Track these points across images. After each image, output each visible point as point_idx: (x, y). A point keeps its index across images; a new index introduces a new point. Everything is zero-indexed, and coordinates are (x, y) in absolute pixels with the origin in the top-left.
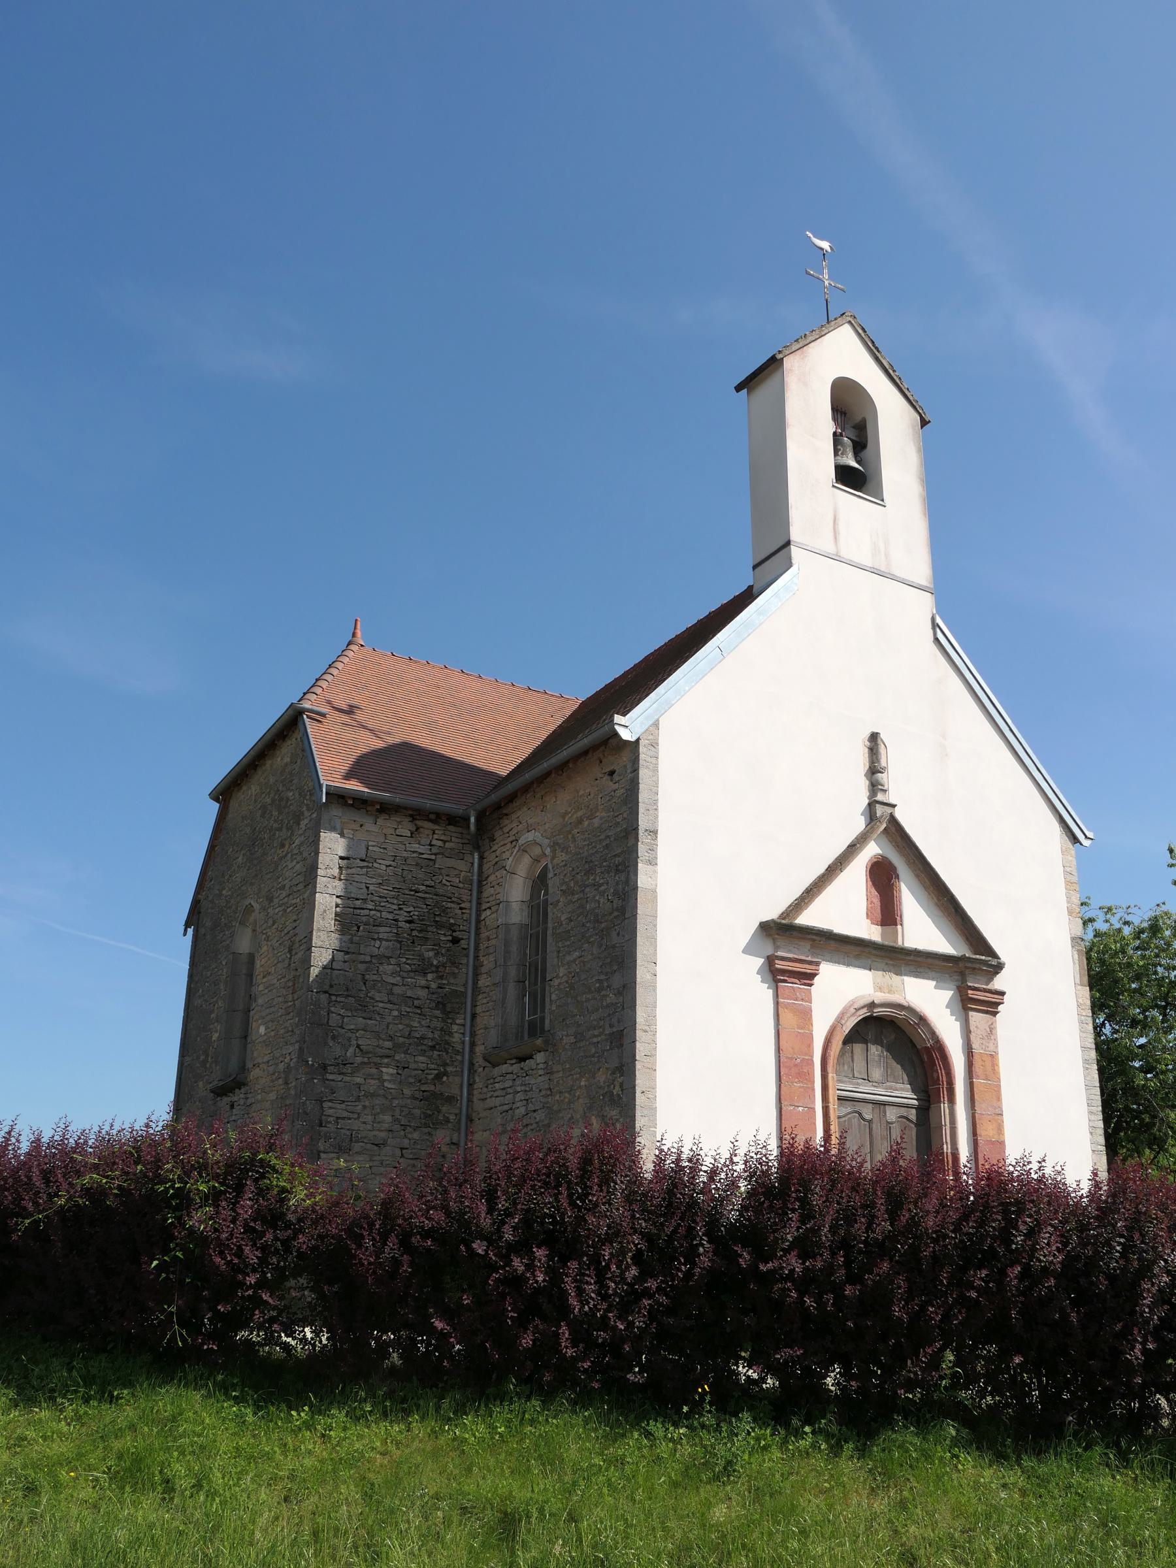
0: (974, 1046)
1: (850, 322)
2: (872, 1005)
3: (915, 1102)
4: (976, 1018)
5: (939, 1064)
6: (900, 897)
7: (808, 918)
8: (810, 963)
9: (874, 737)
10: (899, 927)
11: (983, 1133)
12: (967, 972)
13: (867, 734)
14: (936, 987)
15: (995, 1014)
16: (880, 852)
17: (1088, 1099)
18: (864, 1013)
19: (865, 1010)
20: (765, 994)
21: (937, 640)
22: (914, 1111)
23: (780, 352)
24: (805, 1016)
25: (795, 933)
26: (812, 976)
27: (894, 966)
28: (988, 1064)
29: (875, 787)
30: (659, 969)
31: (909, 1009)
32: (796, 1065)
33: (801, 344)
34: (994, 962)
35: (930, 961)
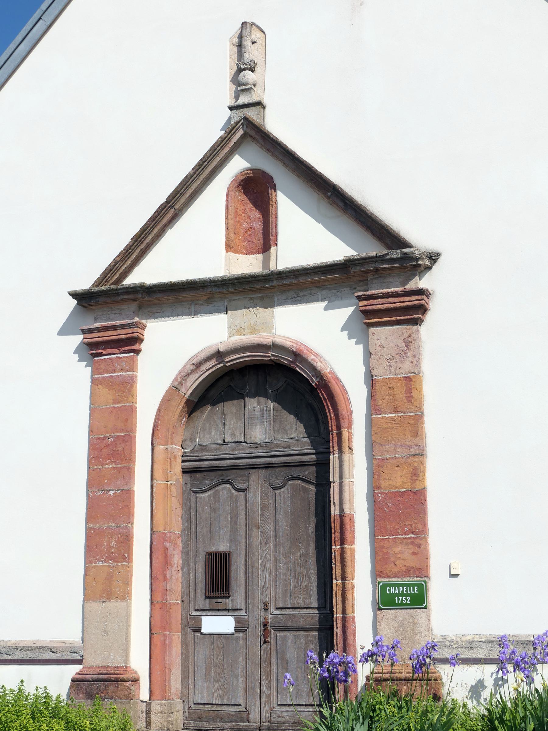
0: (375, 372)
2: (219, 355)
3: (314, 457)
5: (328, 405)
6: (276, 211)
8: (125, 326)
10: (273, 249)
11: (383, 484)
12: (370, 277)
14: (326, 309)
15: (417, 322)
16: (248, 165)
19: (213, 362)
20: (83, 373)
22: (313, 469)
24: (126, 388)
25: (101, 300)
26: (139, 340)
27: (262, 298)
28: (400, 392)
29: (240, 86)
31: (275, 346)
32: (108, 446)
34: (396, 254)
35: (302, 279)
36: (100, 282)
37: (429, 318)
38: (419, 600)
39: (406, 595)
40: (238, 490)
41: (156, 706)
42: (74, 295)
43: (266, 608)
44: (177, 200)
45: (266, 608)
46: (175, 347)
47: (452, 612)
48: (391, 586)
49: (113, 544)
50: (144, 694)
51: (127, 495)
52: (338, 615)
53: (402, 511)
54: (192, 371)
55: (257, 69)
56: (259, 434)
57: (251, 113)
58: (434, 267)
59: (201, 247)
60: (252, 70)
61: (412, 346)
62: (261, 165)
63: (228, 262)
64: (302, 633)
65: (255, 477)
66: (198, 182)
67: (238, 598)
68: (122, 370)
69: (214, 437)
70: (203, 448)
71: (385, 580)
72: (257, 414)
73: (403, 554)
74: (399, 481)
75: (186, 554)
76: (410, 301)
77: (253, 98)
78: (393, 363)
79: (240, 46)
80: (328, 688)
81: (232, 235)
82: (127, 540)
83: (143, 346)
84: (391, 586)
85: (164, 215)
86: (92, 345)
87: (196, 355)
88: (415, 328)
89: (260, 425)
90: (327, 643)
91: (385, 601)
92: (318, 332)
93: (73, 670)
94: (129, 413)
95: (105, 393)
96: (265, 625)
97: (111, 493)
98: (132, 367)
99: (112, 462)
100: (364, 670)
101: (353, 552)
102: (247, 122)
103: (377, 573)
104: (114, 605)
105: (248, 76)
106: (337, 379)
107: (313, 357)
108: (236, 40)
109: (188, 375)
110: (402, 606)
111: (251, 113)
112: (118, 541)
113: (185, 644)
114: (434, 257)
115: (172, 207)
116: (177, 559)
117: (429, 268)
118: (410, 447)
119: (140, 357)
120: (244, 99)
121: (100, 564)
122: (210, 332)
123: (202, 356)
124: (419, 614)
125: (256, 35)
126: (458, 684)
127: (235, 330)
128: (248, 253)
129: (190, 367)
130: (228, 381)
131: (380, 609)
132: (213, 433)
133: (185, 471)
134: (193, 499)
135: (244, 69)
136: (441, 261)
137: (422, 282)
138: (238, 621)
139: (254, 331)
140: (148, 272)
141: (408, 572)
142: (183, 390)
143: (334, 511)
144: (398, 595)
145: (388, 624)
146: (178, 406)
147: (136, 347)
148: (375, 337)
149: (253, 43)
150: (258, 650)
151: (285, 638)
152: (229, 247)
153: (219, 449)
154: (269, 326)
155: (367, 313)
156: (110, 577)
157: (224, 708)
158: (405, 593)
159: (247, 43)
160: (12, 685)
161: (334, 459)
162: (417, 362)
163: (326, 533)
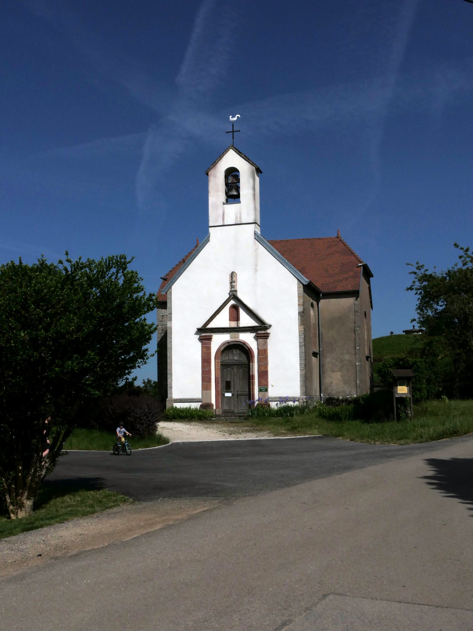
2: (228, 343)
4: (260, 340)
7: (209, 326)
8: (209, 336)
9: (233, 273)
15: (267, 339)
20: (199, 345)
21: (255, 238)
24: (209, 348)
29: (232, 287)
30: (173, 344)
31: (240, 342)
34: (263, 326)
36: (203, 327)
38: (266, 390)
41: (217, 410)
43: (238, 391)
45: (238, 391)
46: (218, 341)
47: (272, 392)
50: (215, 408)
52: (252, 393)
53: (264, 374)
56: (236, 358)
57: (234, 293)
59: (223, 320)
62: (236, 305)
63: (230, 324)
67: (232, 390)
70: (225, 360)
75: (221, 381)
76: (266, 335)
79: (232, 277)
80: (250, 406)
86: (201, 339)
89: (236, 356)
90: (250, 399)
91: (260, 390)
92: (248, 339)
93: (200, 403)
94: (210, 354)
95: (205, 349)
98: (210, 344)
100: (257, 403)
102: (234, 295)
103: (259, 385)
104: (208, 391)
105: (234, 284)
111: (234, 293)
113: (222, 399)
114: (270, 326)
116: (220, 382)
120: (233, 289)
122: (226, 338)
124: (266, 393)
125: (235, 275)
126: (273, 405)
127: (231, 338)
128: (234, 321)
133: (221, 365)
137: (268, 331)
138: (232, 394)
140: (212, 325)
143: (251, 374)
146: (220, 353)
150: (236, 399)
152: (230, 320)
154: (238, 337)
155: (258, 337)
158: (264, 388)
159: (233, 277)
160: (189, 406)
161: (251, 364)
162: (267, 347)
163: (250, 378)
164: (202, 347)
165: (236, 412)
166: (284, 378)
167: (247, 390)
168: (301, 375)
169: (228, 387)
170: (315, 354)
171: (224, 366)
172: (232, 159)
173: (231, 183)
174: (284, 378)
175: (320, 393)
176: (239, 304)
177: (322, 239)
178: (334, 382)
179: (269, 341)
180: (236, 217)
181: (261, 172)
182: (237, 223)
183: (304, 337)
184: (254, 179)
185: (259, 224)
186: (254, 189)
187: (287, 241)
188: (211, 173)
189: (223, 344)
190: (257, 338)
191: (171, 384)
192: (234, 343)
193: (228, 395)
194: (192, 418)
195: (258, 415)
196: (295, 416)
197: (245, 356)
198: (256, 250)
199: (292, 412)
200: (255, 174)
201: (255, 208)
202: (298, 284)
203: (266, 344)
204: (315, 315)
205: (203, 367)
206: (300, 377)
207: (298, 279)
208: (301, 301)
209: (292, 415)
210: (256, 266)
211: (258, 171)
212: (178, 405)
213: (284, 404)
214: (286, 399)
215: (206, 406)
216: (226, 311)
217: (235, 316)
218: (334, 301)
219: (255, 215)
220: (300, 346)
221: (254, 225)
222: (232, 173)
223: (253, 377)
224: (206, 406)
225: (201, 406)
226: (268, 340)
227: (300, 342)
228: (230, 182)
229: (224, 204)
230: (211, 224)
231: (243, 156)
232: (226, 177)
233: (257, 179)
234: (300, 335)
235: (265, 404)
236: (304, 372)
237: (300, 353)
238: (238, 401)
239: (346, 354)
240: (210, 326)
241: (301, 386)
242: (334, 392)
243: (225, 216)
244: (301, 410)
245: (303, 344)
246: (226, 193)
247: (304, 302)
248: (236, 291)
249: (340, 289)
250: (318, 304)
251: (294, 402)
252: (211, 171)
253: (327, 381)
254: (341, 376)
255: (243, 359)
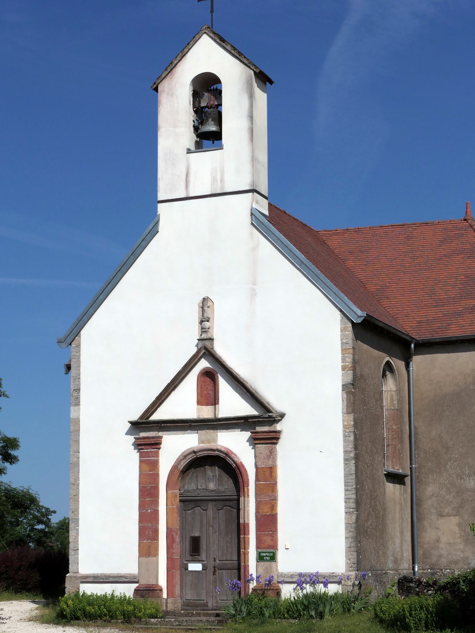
0: (258, 464)
1: (205, 33)
2: (194, 452)
4: (262, 447)
6: (218, 388)
8: (153, 438)
9: (205, 300)
10: (217, 405)
13: (201, 299)
17: (345, 482)
18: (193, 456)
20: (135, 456)
21: (252, 224)
23: (154, 84)
26: (160, 444)
28: (267, 473)
30: (81, 455)
31: (218, 450)
32: (147, 490)
33: (169, 70)
34: (266, 415)
36: (141, 417)
37: (280, 441)
38: (273, 558)
39: (268, 556)
40: (203, 510)
41: (170, 601)
42: (130, 422)
43: (215, 560)
44: (175, 382)
45: (215, 560)
46: (175, 448)
47: (286, 563)
48: (262, 552)
49: (150, 533)
50: (165, 595)
51: (156, 512)
52: (242, 564)
53: (268, 522)
54: (183, 459)
55: (210, 320)
56: (212, 486)
57: (207, 344)
58: (340, 341)
60: (208, 321)
61: (273, 454)
62: (211, 369)
63: (198, 410)
64: (229, 571)
65: (210, 505)
66: (185, 374)
67: (203, 556)
68: (153, 457)
69: (192, 486)
70: (188, 491)
71: (260, 550)
72: (211, 477)
73: (268, 540)
74: (266, 510)
75: (182, 537)
77: (209, 335)
78: (265, 460)
81: (200, 398)
82: (156, 531)
83: (161, 446)
84: (262, 552)
85: (170, 388)
86: (139, 445)
87: (185, 452)
88: (274, 446)
89: (211, 482)
91: (260, 558)
92: (236, 444)
93: (135, 586)
94: (156, 476)
95: (146, 467)
96: (214, 567)
97: (149, 511)
98: (157, 455)
99: (149, 498)
101: (248, 538)
102: (205, 348)
103: (258, 547)
104: (151, 559)
106: (243, 466)
107: (233, 456)
108: (201, 305)
109: (181, 460)
110: (267, 560)
112: (152, 532)
113: (181, 575)
114: (282, 416)
115: (173, 384)
116: (178, 539)
117: (280, 420)
118: (271, 496)
119: (160, 451)
120: (204, 336)
121: (145, 541)
123: (187, 453)
124: (273, 564)
125: (209, 304)
126: (288, 592)
127: (201, 441)
128: (207, 405)
129: (182, 457)
130: (198, 462)
131: (258, 562)
132: (193, 485)
133: (181, 501)
134: (184, 513)
135: (204, 321)
136: (286, 417)
137: (278, 427)
138: (203, 566)
139: (209, 442)
141: (270, 547)
142: (179, 467)
143: (241, 521)
144: (265, 556)
145: (261, 568)
146: (177, 473)
147: (158, 447)
148: (258, 449)
149: (208, 307)
150: (212, 577)
151: (222, 573)
152: (199, 403)
153: (195, 492)
154: (215, 440)
155: (255, 439)
156: (149, 547)
157: (198, 601)
158: (268, 554)
159: (206, 308)
160: (109, 592)
161: (242, 499)
163: (240, 530)
164: (141, 461)
165: (210, 604)
166: (312, 533)
167: (235, 558)
168: (347, 525)
169: (195, 548)
170: (395, 478)
171: (187, 503)
172: (206, 56)
173: (207, 107)
174: (312, 533)
175: (414, 563)
176: (216, 368)
177: (432, 224)
178: (444, 539)
179: (281, 448)
180: (214, 180)
181: (271, 82)
182: (214, 192)
183: (356, 439)
184: (251, 96)
185: (265, 191)
186: (251, 117)
187: (357, 231)
188: (164, 86)
189: (185, 456)
190: (255, 441)
191: (77, 542)
192: (206, 453)
193: (195, 567)
194: (112, 617)
195: (249, 613)
196: (327, 616)
197: (231, 481)
198: (254, 249)
199: (321, 609)
200: (255, 85)
201: (254, 159)
202: (341, 321)
203: (272, 455)
204: (399, 391)
205: (142, 506)
206: (346, 528)
207: (341, 311)
208: (349, 359)
209: (321, 615)
210: (254, 283)
211: (263, 79)
212: (88, 589)
213: (308, 589)
214: (314, 579)
215: (147, 591)
216: (190, 384)
217: (209, 396)
218: (442, 359)
219: (255, 172)
220: (346, 460)
221: (250, 194)
222: (207, 86)
223: (246, 526)
224: (147, 591)
225: (136, 591)
226: (278, 446)
227: (345, 452)
228: (203, 104)
229: (189, 151)
230: (161, 197)
231: (228, 47)
232: (196, 95)
233: (261, 97)
234: (345, 436)
235: (269, 588)
236: (354, 517)
237: (346, 476)
238: (215, 582)
239: (469, 476)
240: (157, 416)
241: (348, 549)
242: (444, 561)
243: (192, 179)
244: (345, 604)
245: (352, 455)
246: (196, 129)
247: (355, 362)
248: (211, 339)
249: (454, 332)
250: (407, 366)
251: (326, 585)
252: (164, 81)
253: (428, 535)
254: (459, 525)
255: (228, 485)
